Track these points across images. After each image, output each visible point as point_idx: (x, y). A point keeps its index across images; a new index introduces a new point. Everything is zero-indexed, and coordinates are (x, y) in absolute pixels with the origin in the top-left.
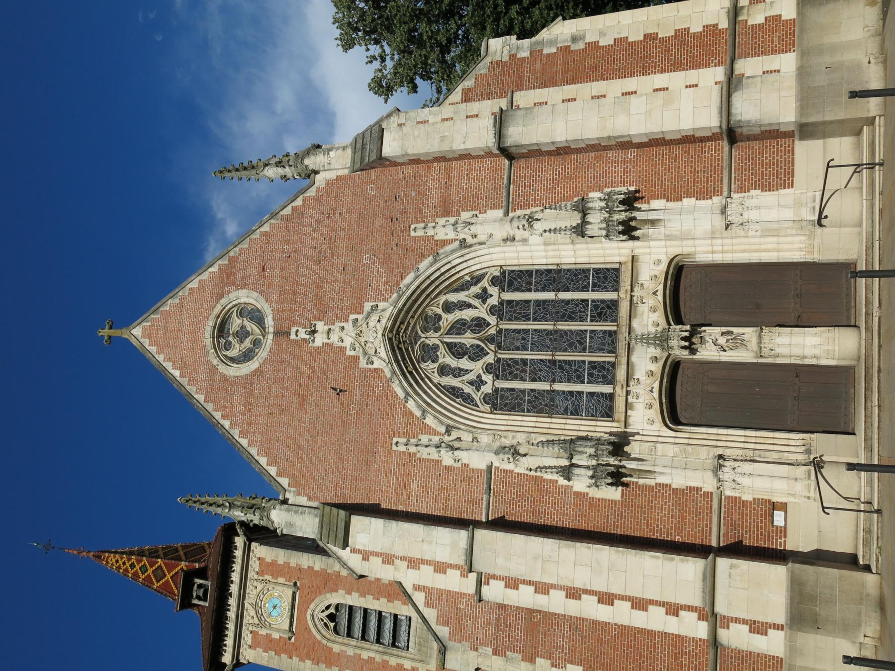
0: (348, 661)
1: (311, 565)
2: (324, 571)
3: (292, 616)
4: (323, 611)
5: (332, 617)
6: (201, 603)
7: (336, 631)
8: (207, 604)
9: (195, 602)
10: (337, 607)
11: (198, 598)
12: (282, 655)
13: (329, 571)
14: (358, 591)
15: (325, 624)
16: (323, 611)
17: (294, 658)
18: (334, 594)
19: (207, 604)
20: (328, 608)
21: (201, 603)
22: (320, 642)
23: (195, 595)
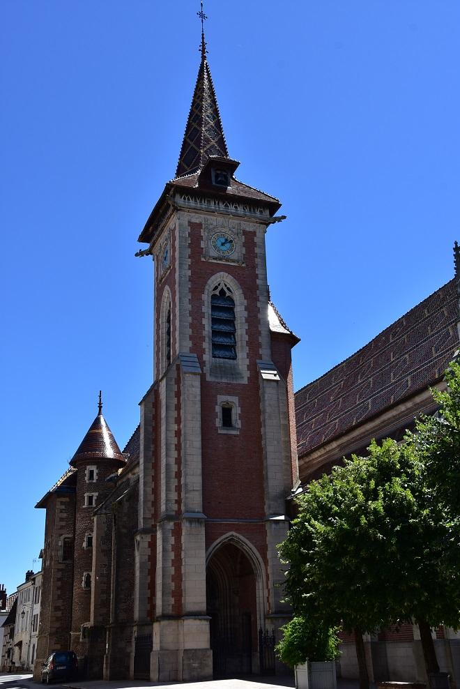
0: (198, 307)
1: (260, 276)
2: (257, 287)
3: (221, 259)
4: (226, 286)
5: (222, 292)
6: (213, 179)
7: (214, 297)
8: (214, 183)
9: (213, 174)
10: (231, 300)
11: (217, 176)
12: (190, 250)
13: (258, 291)
14: (249, 316)
15: (216, 288)
16: (226, 286)
17: (190, 260)
18: (243, 296)
19: (214, 183)
20: (228, 289)
21: (213, 179)
22: (206, 283)
23: (219, 172)
